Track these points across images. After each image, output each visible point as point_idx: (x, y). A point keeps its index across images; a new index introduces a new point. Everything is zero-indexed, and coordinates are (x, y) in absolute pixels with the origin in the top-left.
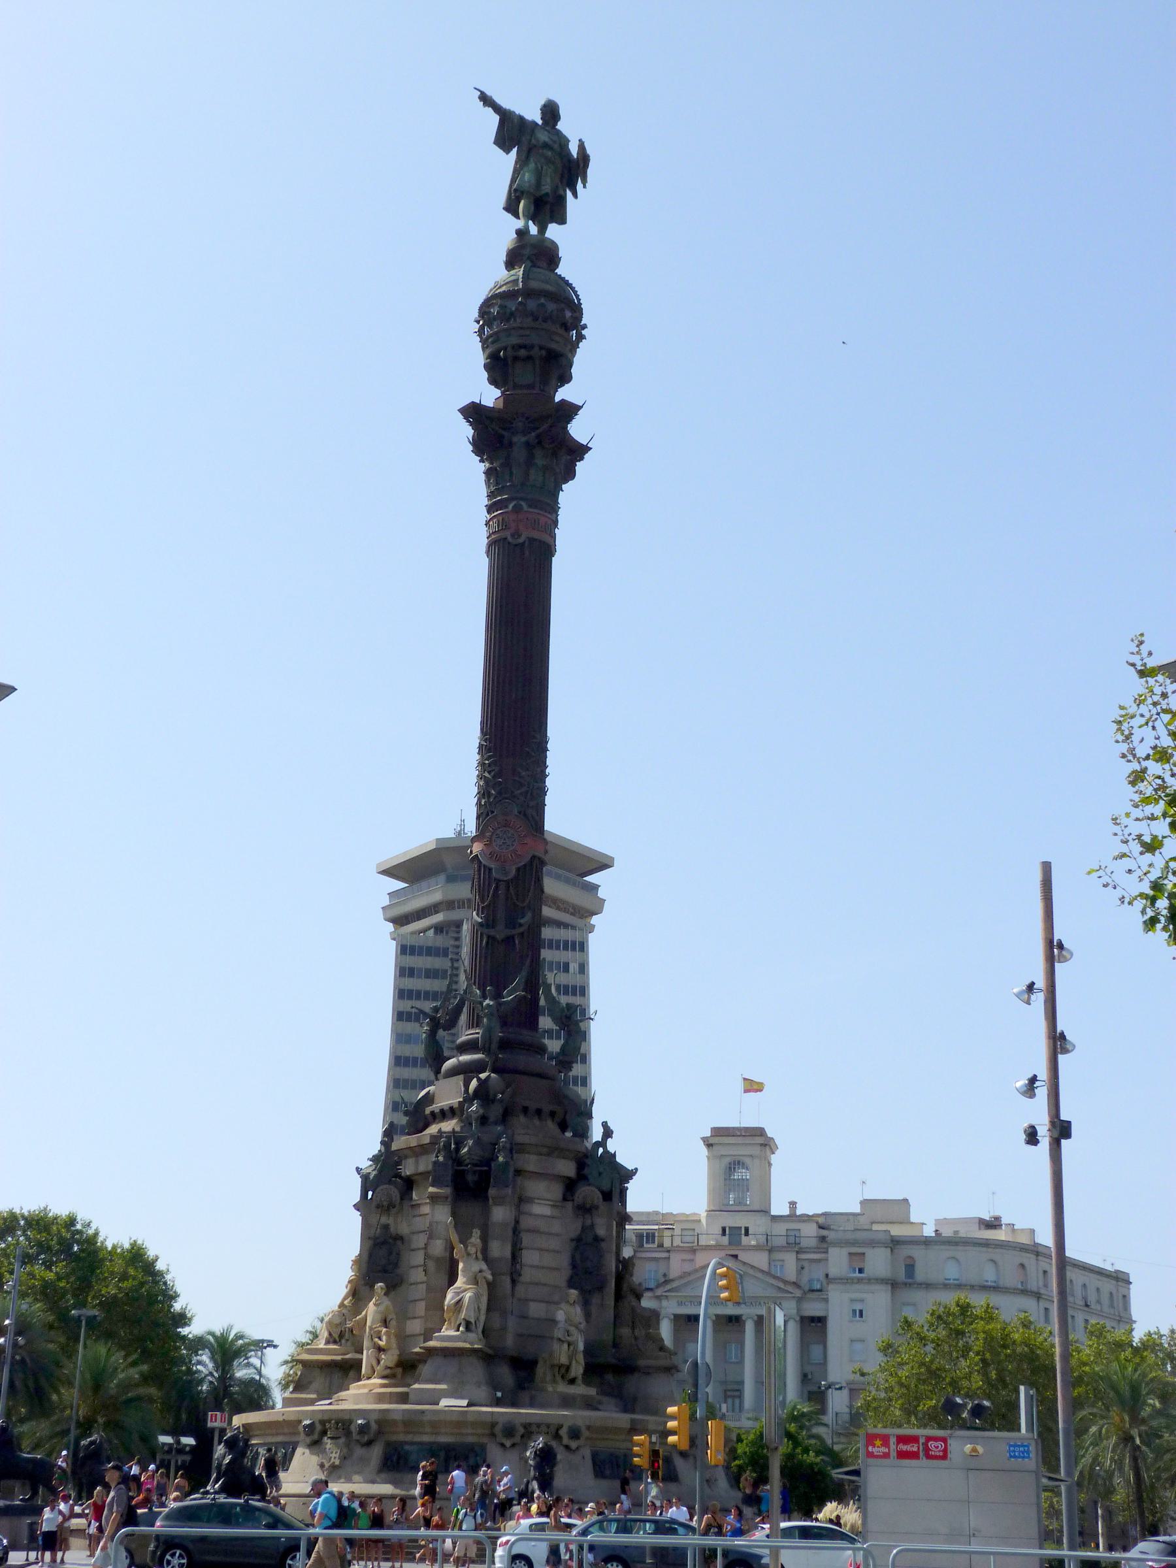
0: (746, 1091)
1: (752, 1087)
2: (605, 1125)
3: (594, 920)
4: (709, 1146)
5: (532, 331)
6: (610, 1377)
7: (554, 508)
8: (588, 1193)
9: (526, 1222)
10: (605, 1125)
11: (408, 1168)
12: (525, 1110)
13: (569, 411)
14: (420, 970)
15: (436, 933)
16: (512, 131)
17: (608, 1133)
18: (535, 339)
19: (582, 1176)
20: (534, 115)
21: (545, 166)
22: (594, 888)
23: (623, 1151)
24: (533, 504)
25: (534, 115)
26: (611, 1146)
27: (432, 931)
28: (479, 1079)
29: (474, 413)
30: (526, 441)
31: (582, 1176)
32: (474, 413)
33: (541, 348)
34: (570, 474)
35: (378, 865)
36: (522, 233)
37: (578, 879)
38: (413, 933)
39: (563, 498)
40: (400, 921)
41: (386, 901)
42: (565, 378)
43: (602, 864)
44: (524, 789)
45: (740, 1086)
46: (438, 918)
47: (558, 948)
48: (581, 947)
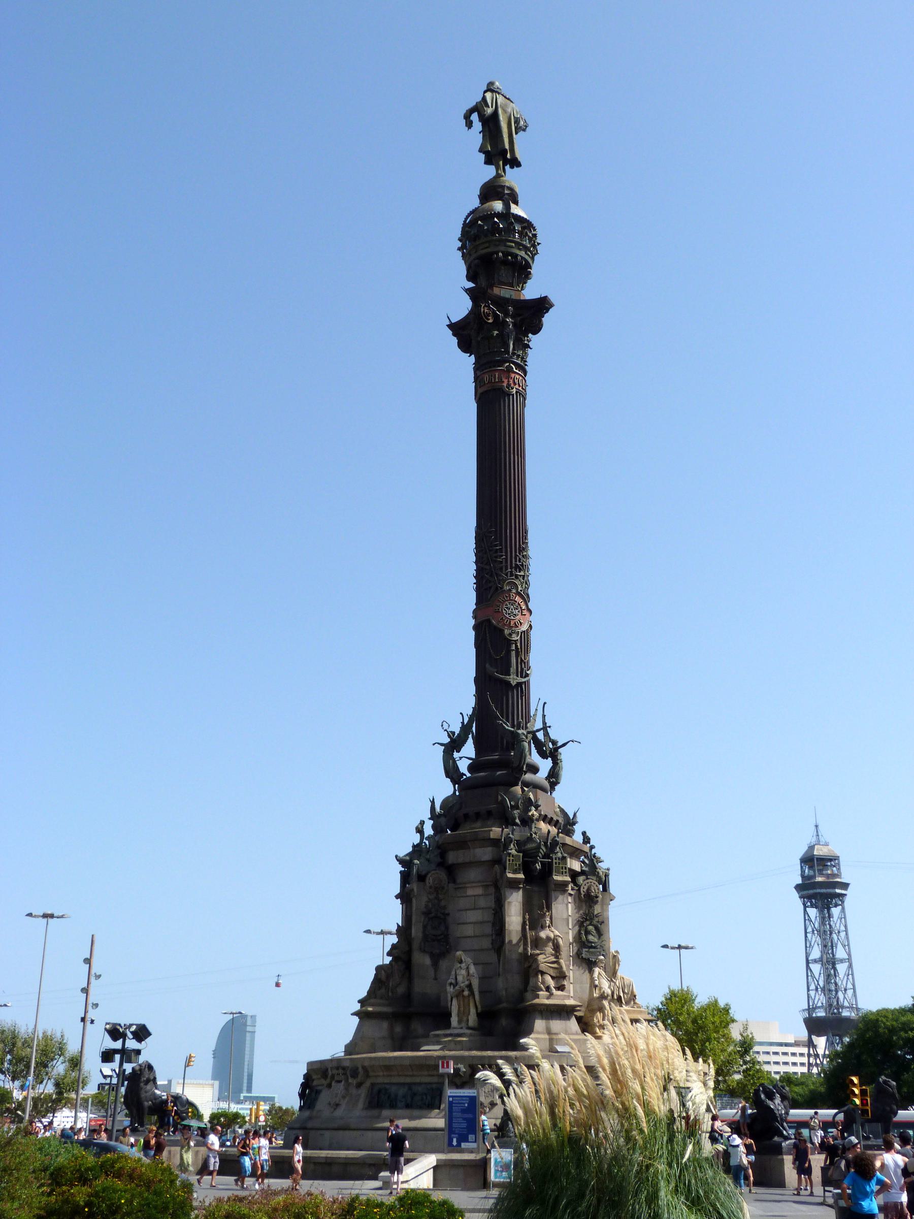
2: (584, 833)
10: (584, 833)
17: (586, 840)
44: (522, 573)
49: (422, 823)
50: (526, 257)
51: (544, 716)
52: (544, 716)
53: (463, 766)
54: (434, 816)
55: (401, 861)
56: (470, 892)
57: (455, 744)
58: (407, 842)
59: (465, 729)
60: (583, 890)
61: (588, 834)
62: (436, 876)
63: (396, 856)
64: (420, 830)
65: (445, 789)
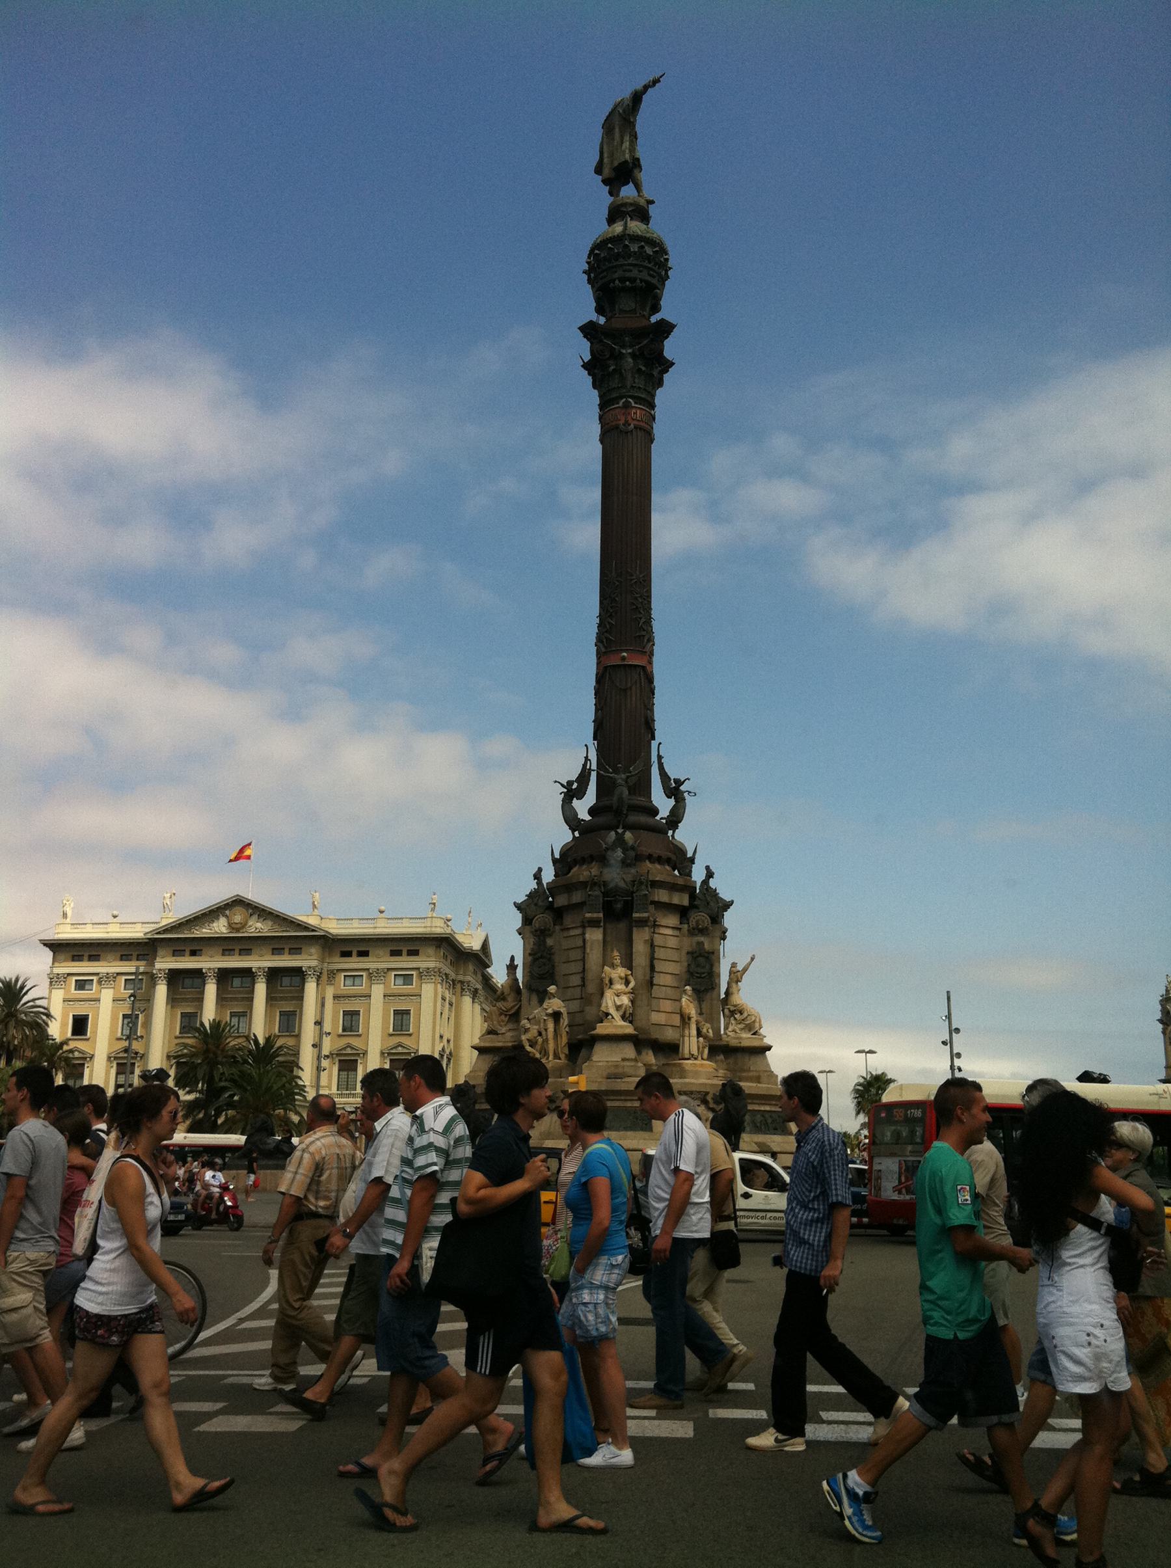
2: (707, 868)
6: (722, 1057)
7: (652, 406)
8: (700, 917)
9: (658, 940)
10: (707, 868)
11: (561, 901)
12: (650, 858)
13: (665, 329)
17: (710, 874)
18: (635, 273)
19: (693, 906)
23: (722, 887)
24: (638, 400)
26: (712, 883)
28: (617, 833)
30: (627, 353)
31: (693, 906)
33: (641, 281)
34: (660, 383)
42: (656, 308)
49: (540, 870)
50: (649, 279)
51: (660, 758)
52: (660, 758)
53: (583, 813)
54: (555, 861)
55: (518, 906)
56: (572, 933)
57: (572, 792)
58: (525, 887)
59: (583, 778)
60: (693, 922)
61: (713, 868)
62: (542, 919)
63: (515, 903)
64: (537, 876)
65: (565, 836)
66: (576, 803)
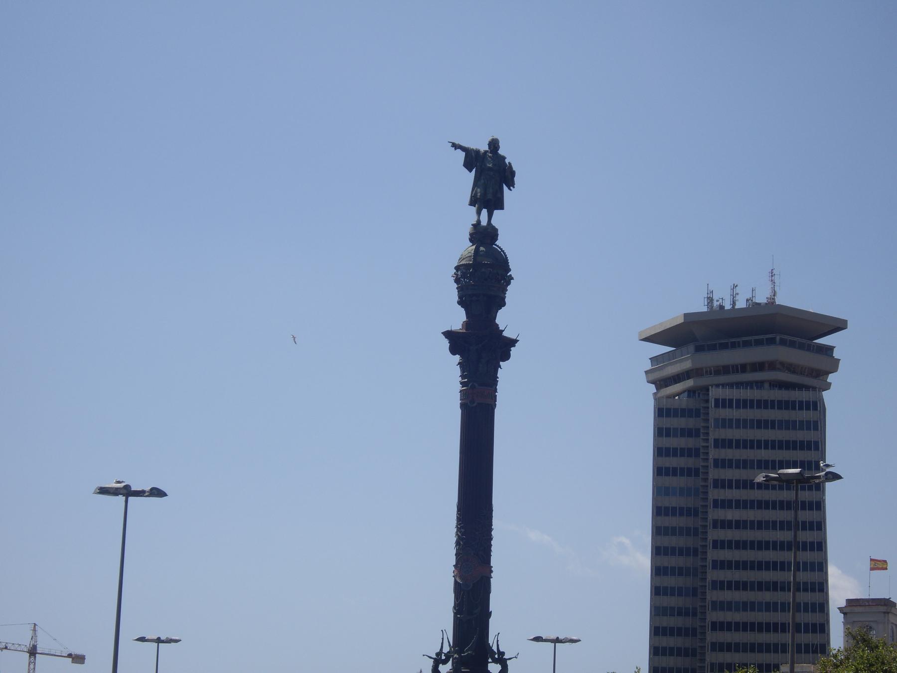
0: (872, 569)
1: (878, 565)
3: (831, 378)
4: (845, 614)
5: (484, 279)
14: (675, 429)
15: (689, 396)
16: (473, 159)
20: (483, 147)
21: (491, 176)
22: (829, 350)
25: (483, 147)
27: (686, 393)
29: (448, 334)
32: (448, 334)
35: (640, 333)
36: (477, 225)
37: (809, 342)
38: (668, 397)
39: (500, 373)
40: (661, 383)
41: (648, 366)
43: (837, 326)
45: (868, 564)
46: (689, 383)
47: (794, 408)
48: (817, 406)
66: (441, 667)
